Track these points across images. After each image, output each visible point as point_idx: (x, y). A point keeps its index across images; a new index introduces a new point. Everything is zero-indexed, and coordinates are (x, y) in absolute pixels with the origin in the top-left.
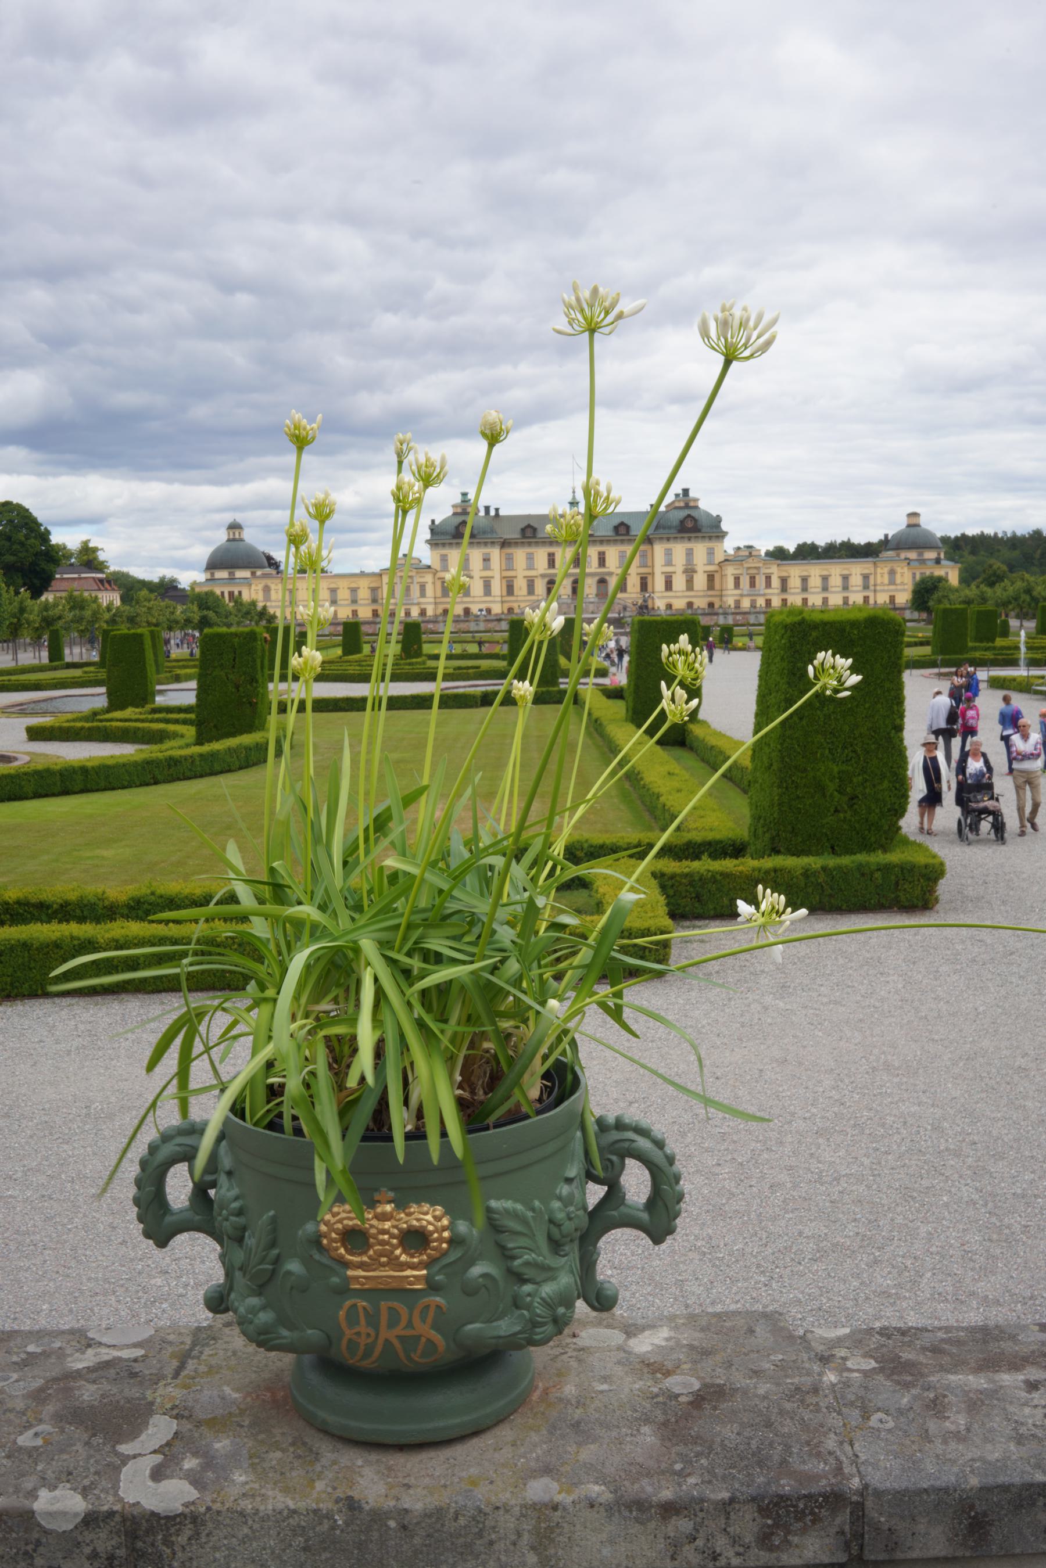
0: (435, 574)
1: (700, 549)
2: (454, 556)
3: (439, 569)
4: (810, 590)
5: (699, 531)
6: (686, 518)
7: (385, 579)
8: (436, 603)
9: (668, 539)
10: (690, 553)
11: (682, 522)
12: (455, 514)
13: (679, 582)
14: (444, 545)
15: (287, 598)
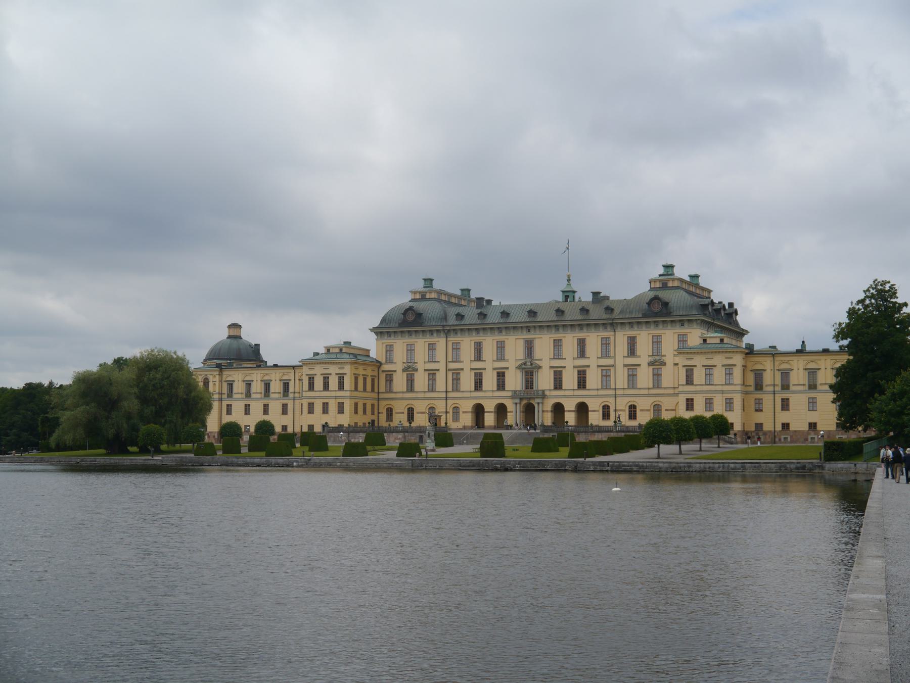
0: (379, 367)
1: (669, 337)
2: (400, 345)
3: (384, 361)
4: (792, 388)
5: (669, 314)
6: (652, 300)
7: (306, 370)
8: (378, 399)
9: (631, 324)
10: (657, 342)
11: (649, 304)
12: (413, 300)
13: (645, 377)
14: (389, 334)
15: (225, 390)
